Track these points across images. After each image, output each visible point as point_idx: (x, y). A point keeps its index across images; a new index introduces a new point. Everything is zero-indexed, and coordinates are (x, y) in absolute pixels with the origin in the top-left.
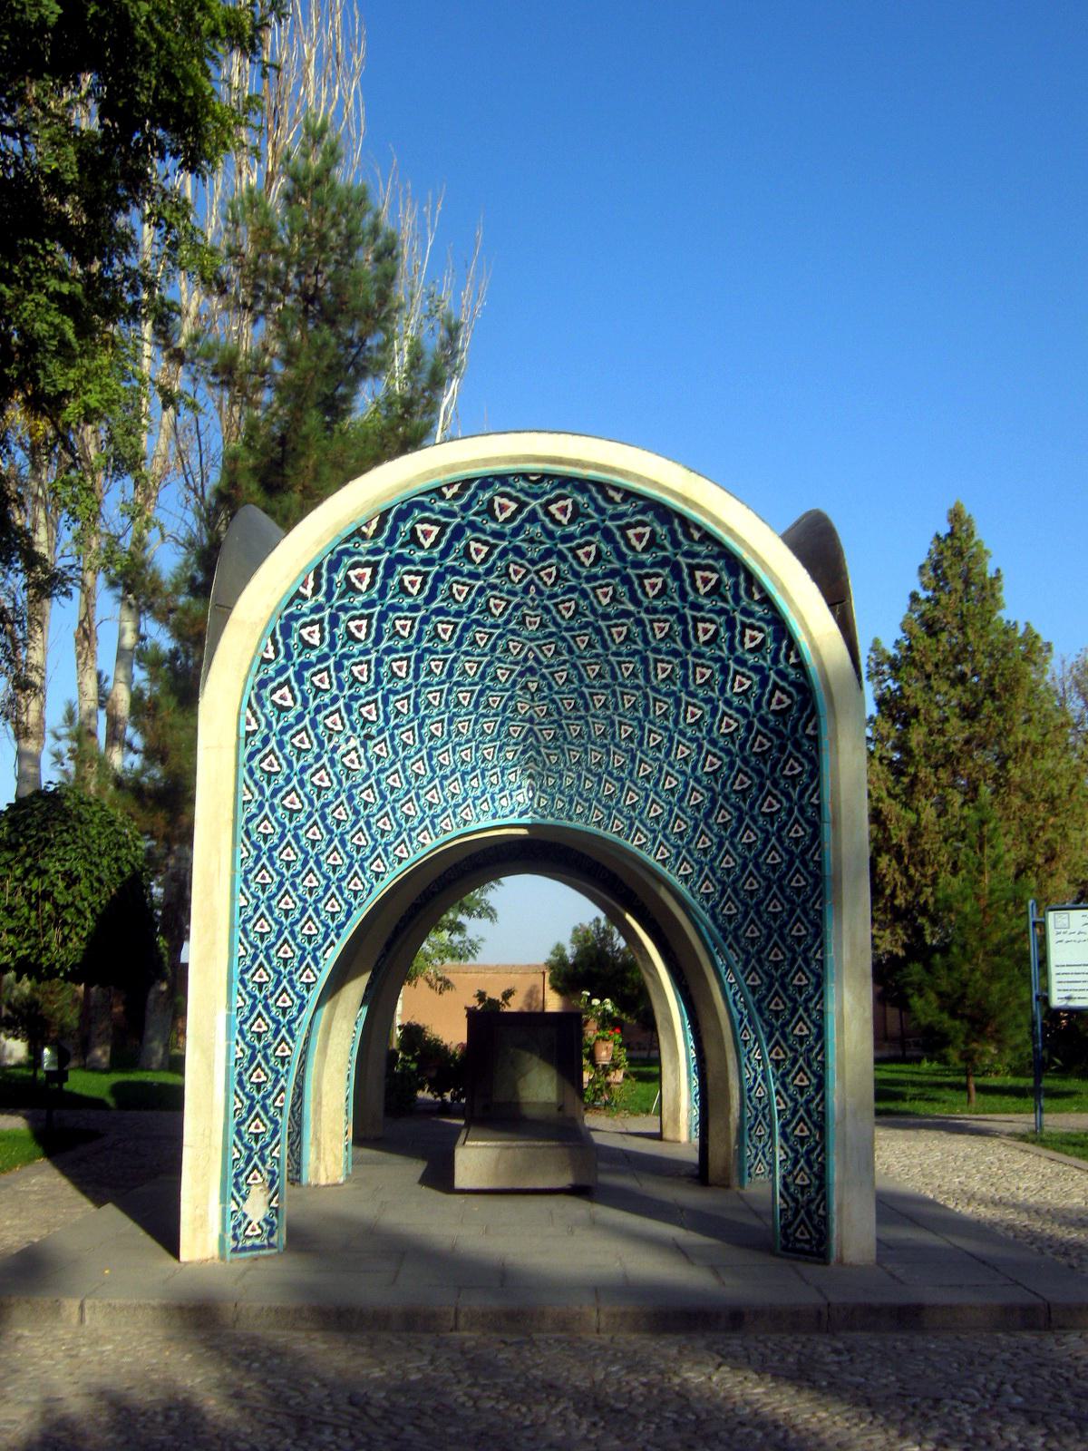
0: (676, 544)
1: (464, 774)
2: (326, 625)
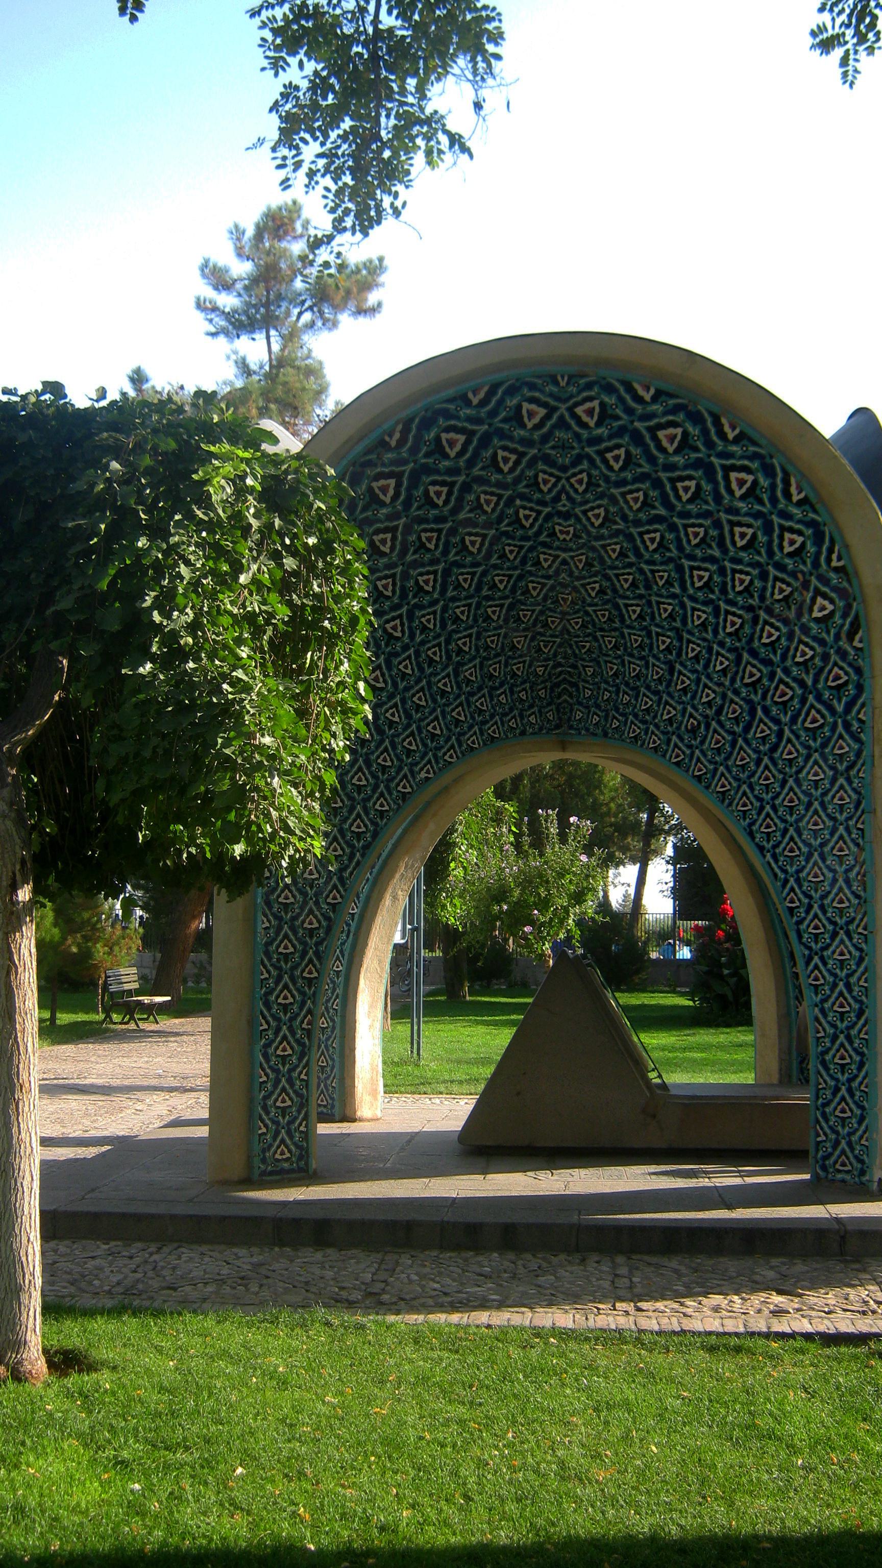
0: (710, 445)
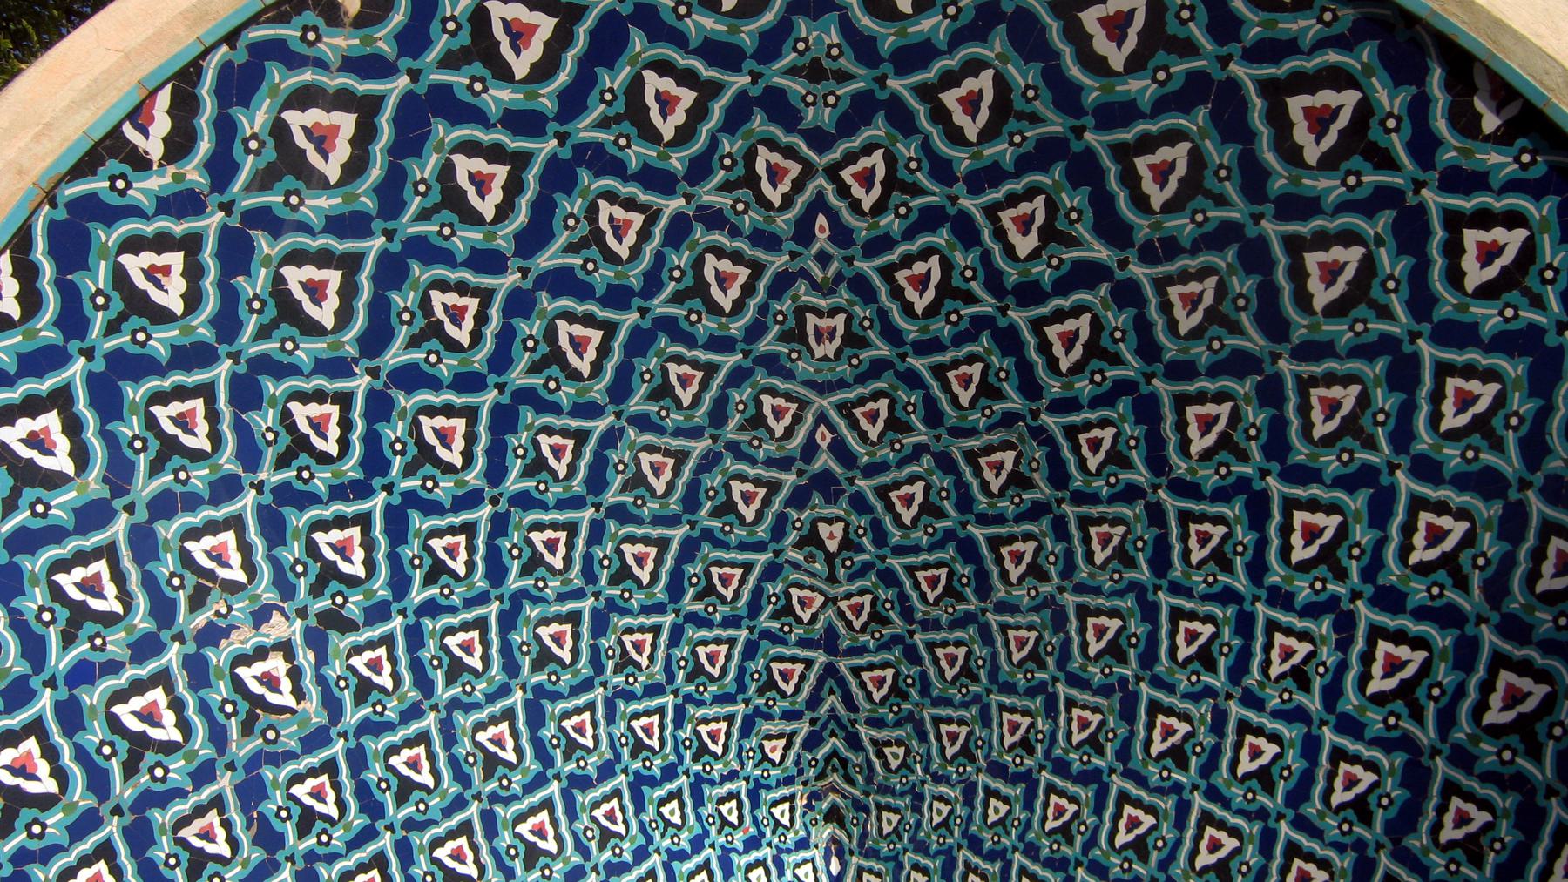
1: (639, 783)
2: (208, 256)
